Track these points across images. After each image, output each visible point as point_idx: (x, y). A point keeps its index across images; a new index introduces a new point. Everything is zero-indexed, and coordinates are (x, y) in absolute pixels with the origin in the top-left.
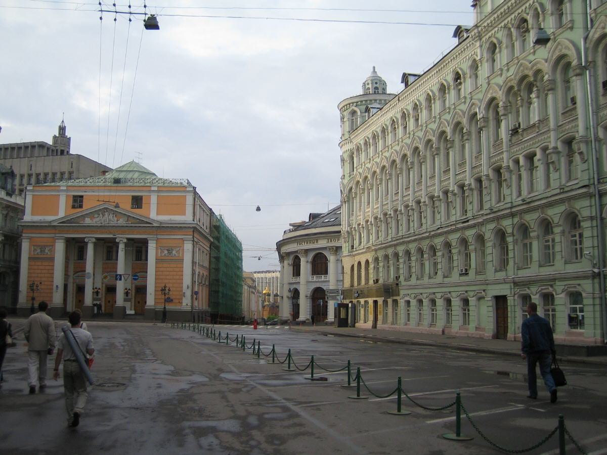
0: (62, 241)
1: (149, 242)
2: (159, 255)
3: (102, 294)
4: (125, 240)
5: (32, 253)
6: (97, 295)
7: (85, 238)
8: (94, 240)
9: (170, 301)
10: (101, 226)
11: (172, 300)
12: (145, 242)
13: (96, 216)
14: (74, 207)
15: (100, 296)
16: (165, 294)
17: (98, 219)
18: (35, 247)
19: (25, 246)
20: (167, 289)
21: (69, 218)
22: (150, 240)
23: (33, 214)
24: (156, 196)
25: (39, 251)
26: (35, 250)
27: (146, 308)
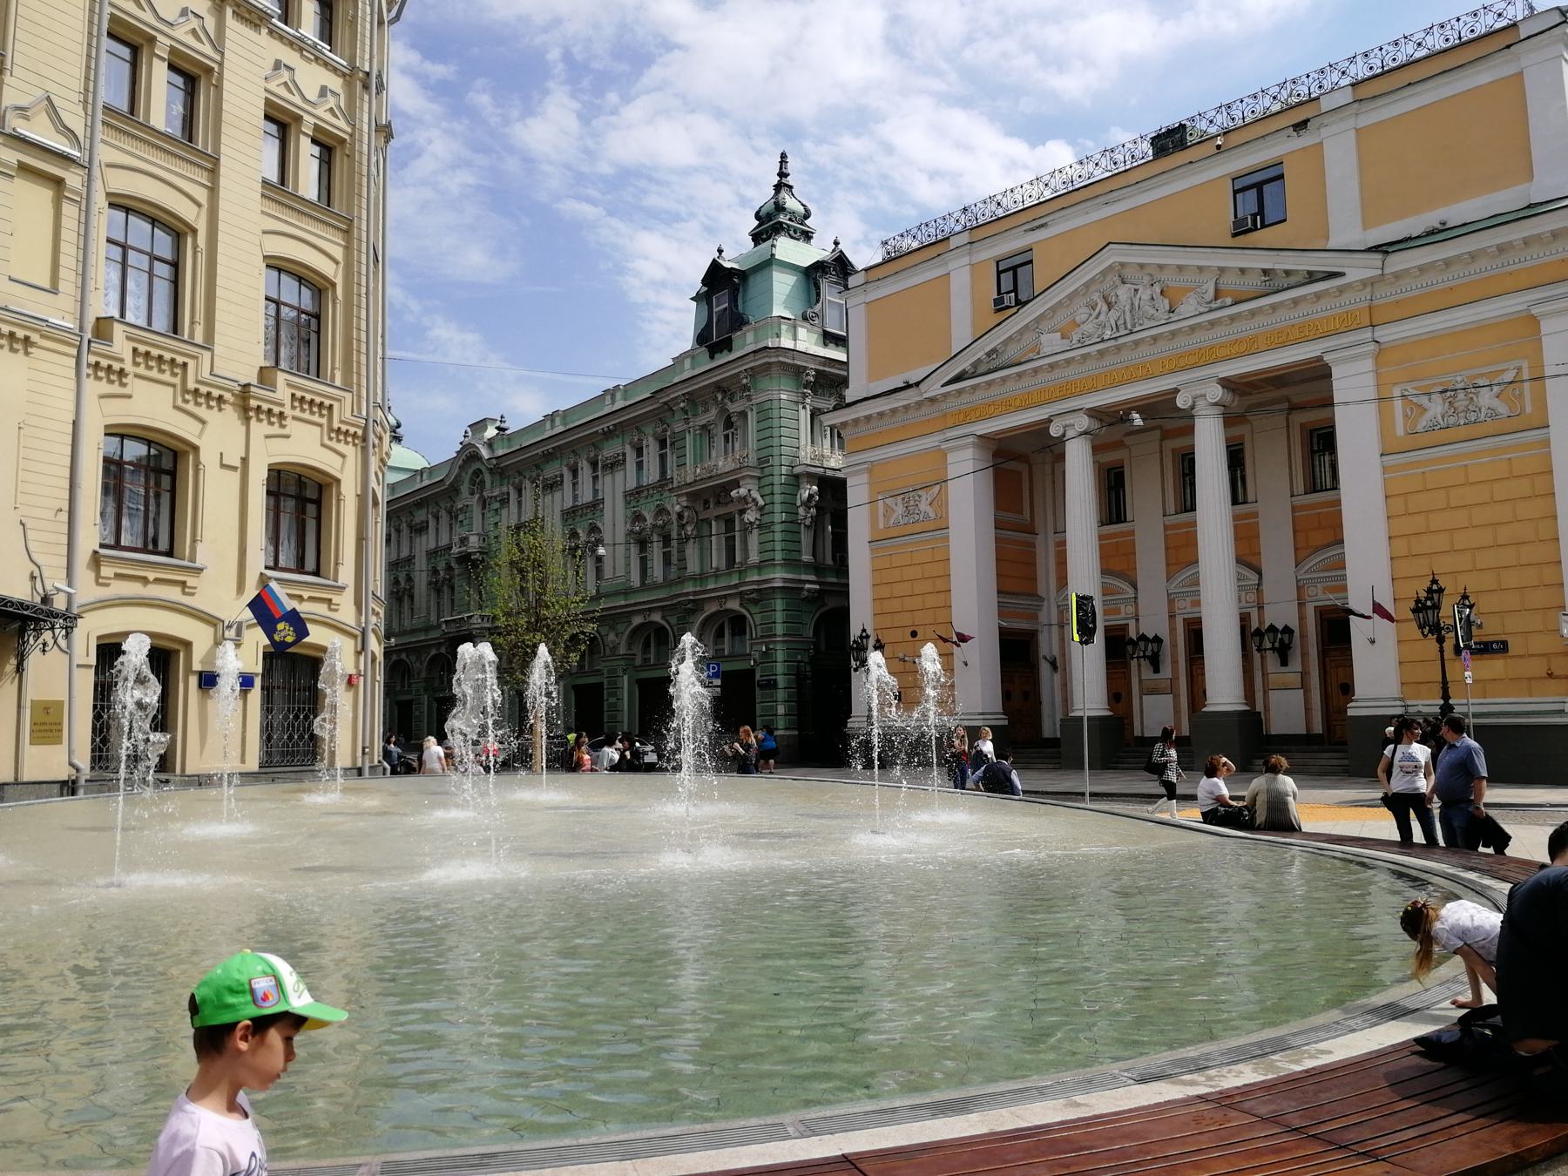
0: (969, 453)
1: (1336, 372)
2: (1400, 431)
3: (1175, 662)
5: (881, 526)
6: (1157, 670)
7: (1049, 421)
8: (1084, 422)
12: (1319, 373)
14: (999, 306)
15: (1166, 672)
18: (890, 501)
19: (857, 493)
21: (981, 354)
22: (1345, 360)
23: (873, 376)
24: (1352, 134)
25: (900, 509)
26: (888, 511)
27: (1350, 713)
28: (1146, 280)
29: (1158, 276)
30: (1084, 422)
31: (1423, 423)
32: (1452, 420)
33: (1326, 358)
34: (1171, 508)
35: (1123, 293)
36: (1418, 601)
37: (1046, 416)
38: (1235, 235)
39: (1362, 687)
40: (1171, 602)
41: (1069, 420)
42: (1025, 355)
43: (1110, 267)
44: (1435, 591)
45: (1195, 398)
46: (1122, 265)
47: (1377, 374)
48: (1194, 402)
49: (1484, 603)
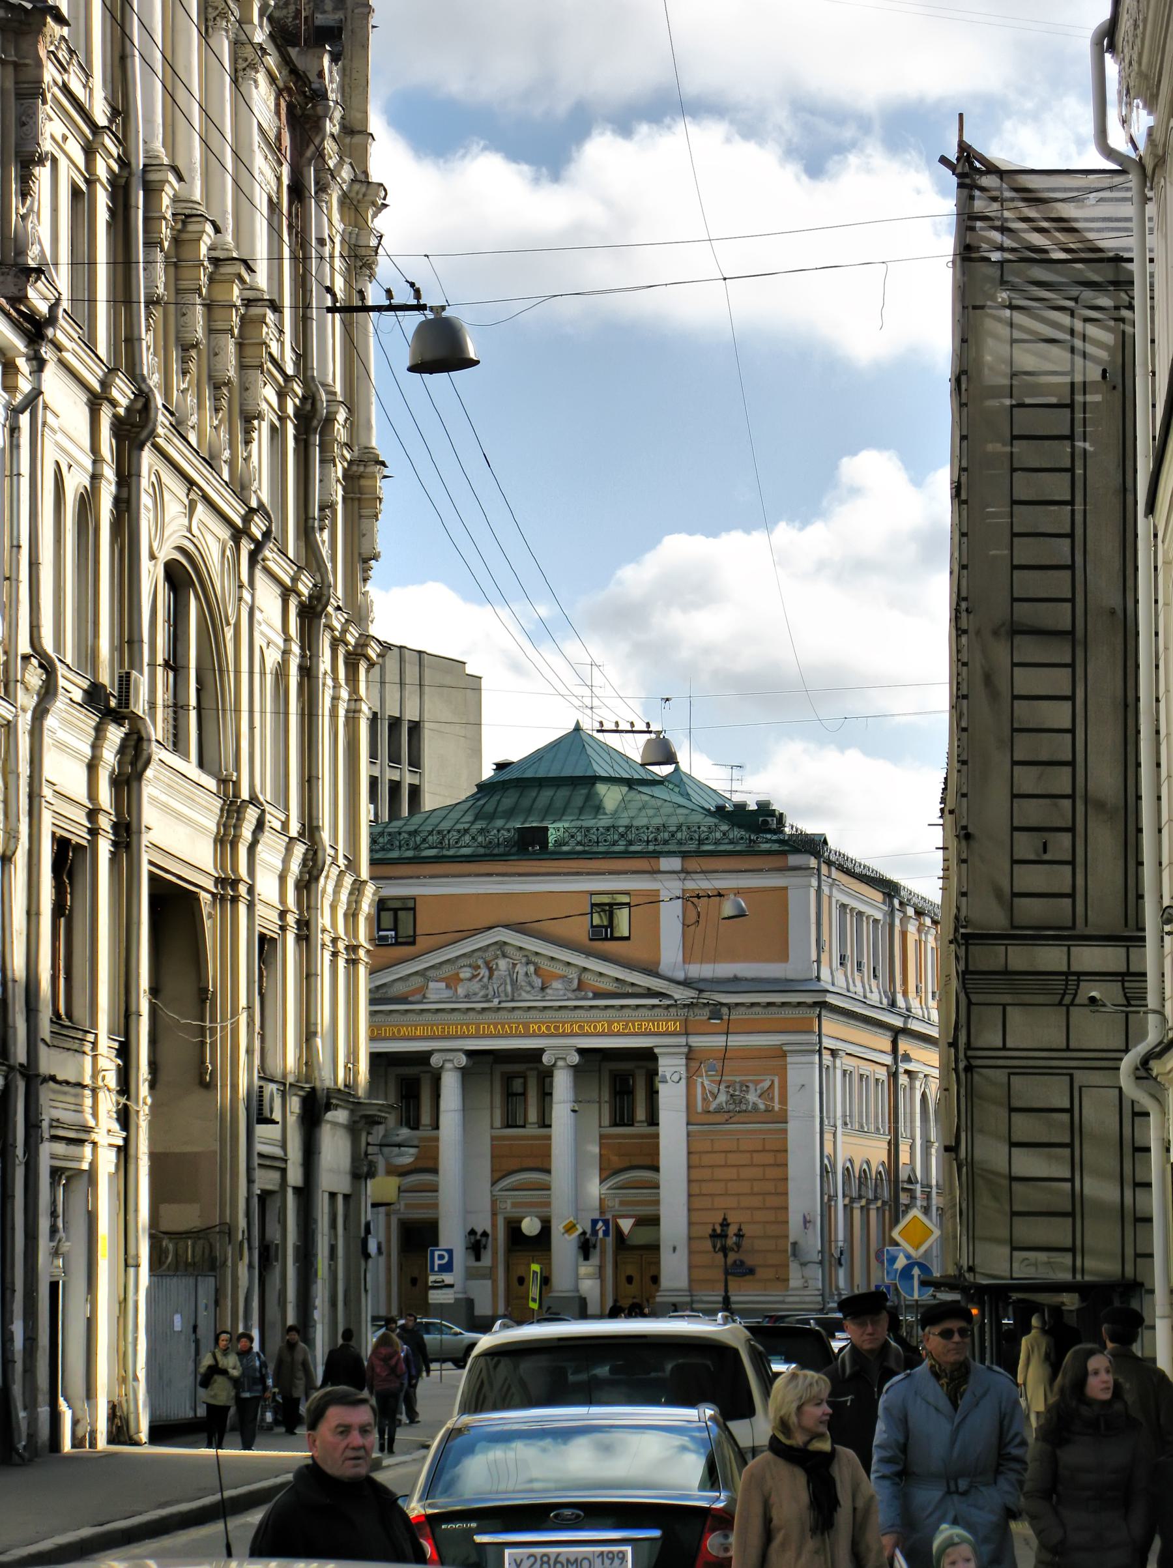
2: (699, 1109)
4: (575, 1059)
9: (744, 1275)
10: (484, 1009)
11: (751, 1271)
13: (465, 973)
16: (725, 1250)
17: (475, 986)
20: (732, 1230)
27: (658, 1299)
28: (524, 960)
29: (534, 959)
30: (463, 1060)
31: (712, 1107)
32: (732, 1107)
33: (656, 1050)
34: (498, 1124)
35: (503, 964)
36: (714, 1230)
37: (430, 1049)
38: (591, 940)
39: (665, 1282)
40: (494, 1202)
41: (450, 1056)
42: (414, 993)
43: (496, 943)
44: (725, 1224)
45: (557, 1059)
46: (505, 943)
47: (687, 1065)
48: (555, 1062)
49: (746, 1230)
